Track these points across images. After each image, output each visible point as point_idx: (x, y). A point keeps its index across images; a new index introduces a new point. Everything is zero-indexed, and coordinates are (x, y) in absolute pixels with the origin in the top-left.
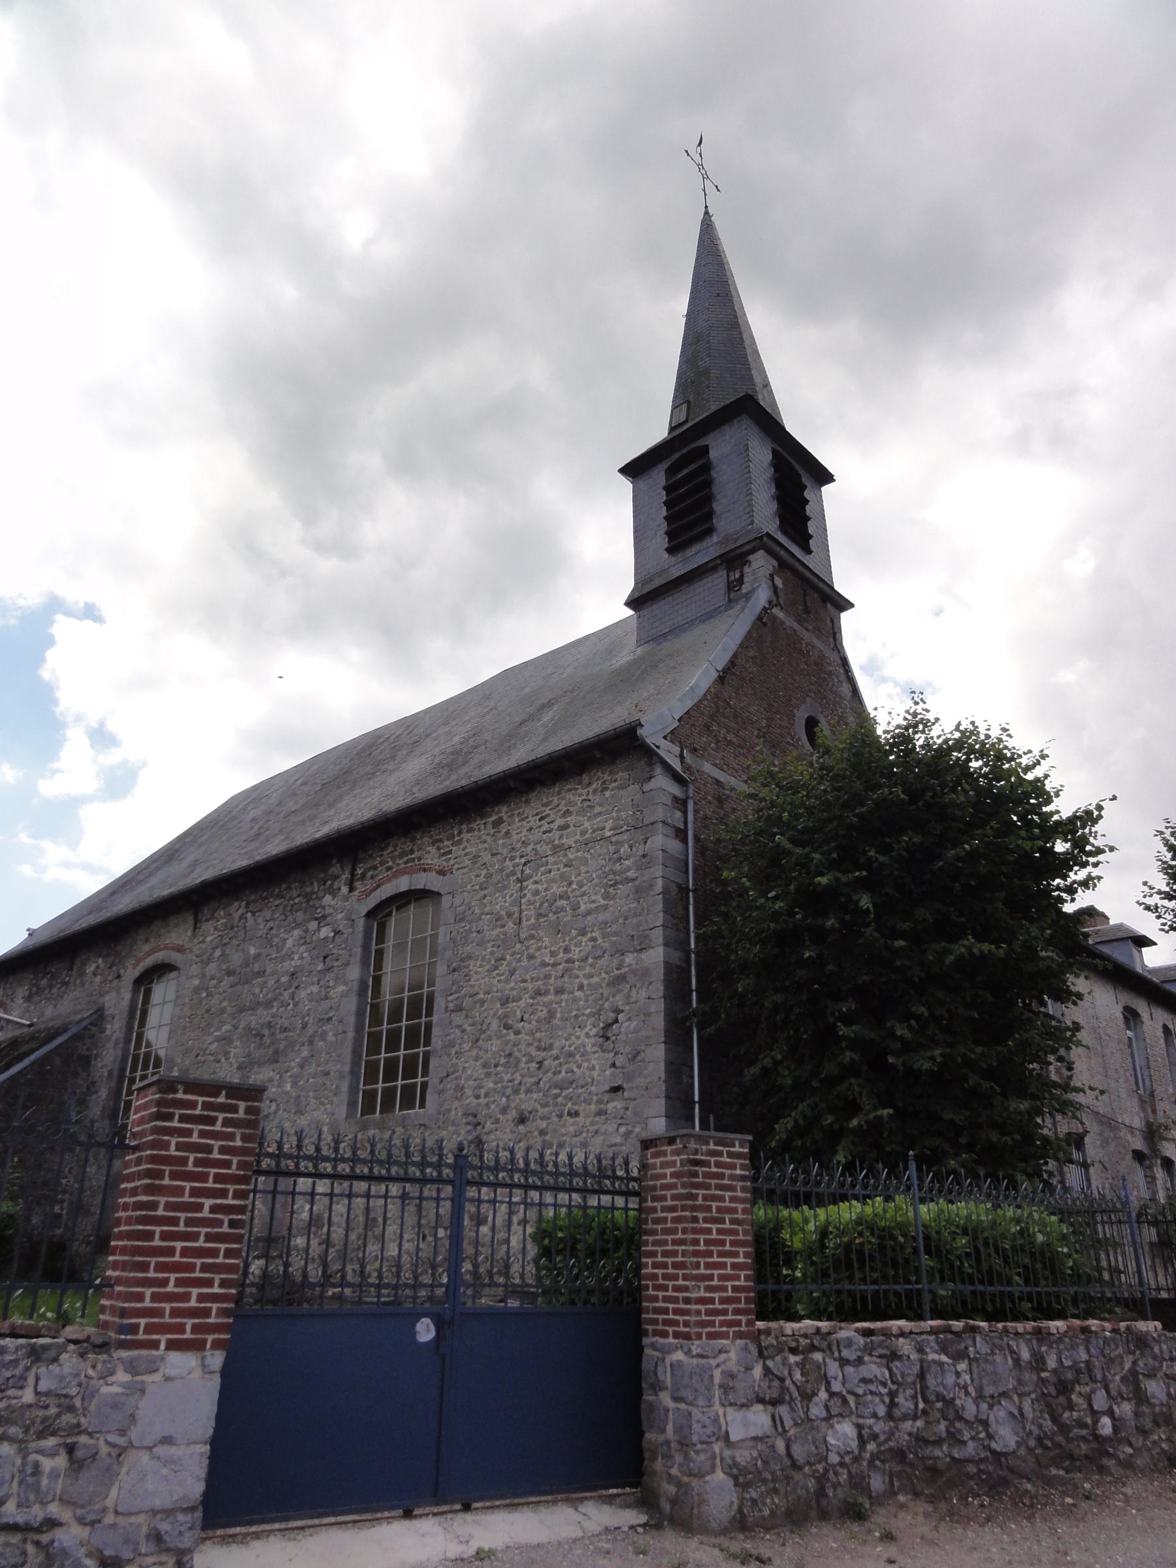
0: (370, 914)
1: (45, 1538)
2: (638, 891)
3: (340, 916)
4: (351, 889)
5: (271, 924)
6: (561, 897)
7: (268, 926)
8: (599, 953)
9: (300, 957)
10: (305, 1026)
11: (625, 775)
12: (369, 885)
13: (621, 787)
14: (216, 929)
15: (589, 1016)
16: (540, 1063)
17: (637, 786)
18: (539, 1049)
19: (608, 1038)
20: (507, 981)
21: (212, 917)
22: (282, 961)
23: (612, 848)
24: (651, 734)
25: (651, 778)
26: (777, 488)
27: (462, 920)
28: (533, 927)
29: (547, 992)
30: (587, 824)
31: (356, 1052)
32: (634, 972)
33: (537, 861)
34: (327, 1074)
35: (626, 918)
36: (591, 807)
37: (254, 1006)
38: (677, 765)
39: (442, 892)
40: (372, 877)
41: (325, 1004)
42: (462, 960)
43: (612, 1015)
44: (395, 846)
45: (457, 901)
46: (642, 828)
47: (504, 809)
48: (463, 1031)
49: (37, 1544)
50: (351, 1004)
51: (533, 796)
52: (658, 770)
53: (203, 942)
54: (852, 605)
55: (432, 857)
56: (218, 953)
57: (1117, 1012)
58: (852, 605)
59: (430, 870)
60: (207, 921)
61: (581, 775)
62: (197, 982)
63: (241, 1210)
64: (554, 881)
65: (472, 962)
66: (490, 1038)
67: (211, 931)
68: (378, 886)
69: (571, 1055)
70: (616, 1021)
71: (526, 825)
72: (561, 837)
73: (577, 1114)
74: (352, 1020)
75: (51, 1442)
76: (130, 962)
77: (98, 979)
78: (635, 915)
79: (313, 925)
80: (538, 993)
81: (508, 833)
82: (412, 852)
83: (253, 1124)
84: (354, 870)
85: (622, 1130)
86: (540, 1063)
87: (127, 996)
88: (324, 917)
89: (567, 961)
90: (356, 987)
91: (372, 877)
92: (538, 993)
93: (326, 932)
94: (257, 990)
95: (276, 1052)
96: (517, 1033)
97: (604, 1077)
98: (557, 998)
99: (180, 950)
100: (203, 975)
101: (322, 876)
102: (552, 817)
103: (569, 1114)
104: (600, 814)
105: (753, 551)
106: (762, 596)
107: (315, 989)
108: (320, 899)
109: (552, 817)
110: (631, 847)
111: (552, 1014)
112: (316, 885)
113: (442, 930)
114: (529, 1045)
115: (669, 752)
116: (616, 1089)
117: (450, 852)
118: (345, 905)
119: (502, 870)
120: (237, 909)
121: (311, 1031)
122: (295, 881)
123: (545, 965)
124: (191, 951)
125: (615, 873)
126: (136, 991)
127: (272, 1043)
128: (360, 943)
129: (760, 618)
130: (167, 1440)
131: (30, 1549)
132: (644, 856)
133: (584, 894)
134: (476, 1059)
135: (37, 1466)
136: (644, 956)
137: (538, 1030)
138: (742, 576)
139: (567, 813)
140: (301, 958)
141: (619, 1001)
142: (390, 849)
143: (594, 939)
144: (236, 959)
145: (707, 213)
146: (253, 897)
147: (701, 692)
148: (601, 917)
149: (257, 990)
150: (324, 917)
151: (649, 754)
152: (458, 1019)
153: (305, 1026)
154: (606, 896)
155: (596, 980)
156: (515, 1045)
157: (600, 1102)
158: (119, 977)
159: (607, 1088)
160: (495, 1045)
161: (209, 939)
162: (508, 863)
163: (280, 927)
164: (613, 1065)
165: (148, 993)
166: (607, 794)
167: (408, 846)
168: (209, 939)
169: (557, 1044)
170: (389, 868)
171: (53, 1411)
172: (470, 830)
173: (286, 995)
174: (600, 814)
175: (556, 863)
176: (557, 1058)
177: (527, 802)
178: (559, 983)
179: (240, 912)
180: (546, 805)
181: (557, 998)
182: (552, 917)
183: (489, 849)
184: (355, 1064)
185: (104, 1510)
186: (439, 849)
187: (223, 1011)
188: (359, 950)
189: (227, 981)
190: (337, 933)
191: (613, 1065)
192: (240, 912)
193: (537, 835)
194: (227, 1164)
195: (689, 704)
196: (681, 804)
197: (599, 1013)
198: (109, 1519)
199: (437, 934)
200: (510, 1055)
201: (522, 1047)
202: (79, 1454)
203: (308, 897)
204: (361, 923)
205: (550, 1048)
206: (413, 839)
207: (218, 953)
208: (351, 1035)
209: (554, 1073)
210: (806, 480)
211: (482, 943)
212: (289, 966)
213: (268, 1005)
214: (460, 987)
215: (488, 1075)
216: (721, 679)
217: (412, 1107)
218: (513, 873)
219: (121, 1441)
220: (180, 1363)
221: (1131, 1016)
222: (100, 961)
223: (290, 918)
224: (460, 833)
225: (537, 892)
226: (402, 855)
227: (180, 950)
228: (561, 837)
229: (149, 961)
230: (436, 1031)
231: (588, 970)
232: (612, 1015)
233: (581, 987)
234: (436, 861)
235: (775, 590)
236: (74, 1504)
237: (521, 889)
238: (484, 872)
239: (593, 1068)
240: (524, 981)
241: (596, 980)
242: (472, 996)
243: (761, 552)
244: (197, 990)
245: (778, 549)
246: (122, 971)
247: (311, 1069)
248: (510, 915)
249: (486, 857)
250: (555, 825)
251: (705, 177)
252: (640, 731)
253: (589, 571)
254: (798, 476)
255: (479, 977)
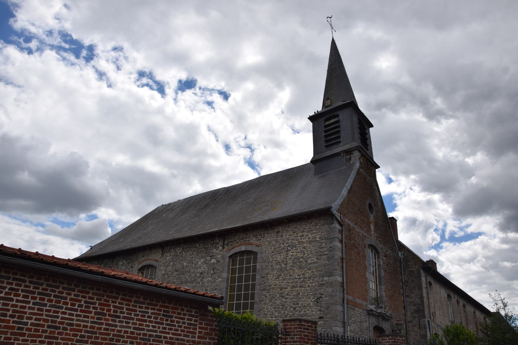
0: (230, 257)
2: (328, 258)
3: (219, 256)
4: (223, 248)
5: (192, 256)
6: (301, 258)
7: (191, 257)
8: (315, 276)
9: (204, 268)
13: (322, 225)
14: (170, 255)
15: (312, 295)
16: (295, 309)
18: (294, 304)
19: (318, 302)
20: (282, 282)
21: (169, 252)
22: (197, 268)
23: (319, 244)
25: (332, 224)
26: (360, 130)
27: (265, 262)
28: (291, 266)
29: (297, 287)
30: (310, 236)
32: (327, 283)
33: (293, 246)
35: (324, 266)
36: (312, 231)
38: (339, 219)
40: (231, 245)
42: (266, 274)
44: (240, 236)
45: (263, 256)
46: (331, 239)
47: (280, 228)
48: (266, 297)
50: (224, 285)
52: (335, 221)
53: (166, 259)
55: (253, 240)
56: (171, 264)
57: (446, 295)
60: (167, 252)
64: (299, 252)
67: (168, 257)
68: (233, 248)
70: (321, 297)
71: (288, 235)
72: (301, 239)
74: (225, 290)
77: (124, 267)
78: (328, 265)
79: (209, 258)
80: (294, 287)
81: (282, 236)
82: (246, 238)
84: (224, 242)
85: (323, 330)
86: (295, 309)
89: (304, 278)
91: (231, 245)
92: (294, 287)
93: (213, 261)
94: (188, 277)
96: (286, 299)
99: (157, 261)
104: (315, 233)
105: (354, 150)
106: (358, 165)
107: (210, 279)
108: (211, 250)
110: (326, 244)
111: (298, 294)
112: (209, 245)
113: (258, 264)
115: (338, 215)
116: (321, 318)
117: (260, 240)
118: (221, 253)
119: (280, 247)
120: (179, 250)
123: (296, 278)
125: (321, 252)
128: (227, 266)
129: (357, 172)
133: (309, 258)
134: (271, 306)
136: (330, 278)
137: (293, 298)
138: (350, 158)
139: (303, 232)
140: (204, 268)
142: (238, 236)
143: (313, 272)
144: (178, 266)
146: (185, 247)
147: (344, 196)
150: (213, 256)
151: (332, 215)
152: (264, 293)
154: (317, 259)
155: (314, 284)
158: (132, 267)
159: (318, 317)
161: (167, 259)
162: (282, 245)
163: (195, 257)
164: (320, 310)
166: (317, 227)
167: (244, 236)
168: (167, 259)
169: (300, 303)
170: (237, 243)
172: (268, 233)
173: (199, 280)
174: (315, 233)
176: (300, 307)
177: (289, 227)
178: (301, 284)
179: (180, 251)
180: (296, 228)
183: (275, 240)
186: (256, 238)
189: (175, 273)
190: (218, 261)
192: (180, 251)
194: (312, 340)
195: (342, 200)
196: (341, 232)
197: (315, 294)
200: (284, 305)
203: (207, 249)
204: (227, 259)
205: (297, 304)
207: (171, 264)
210: (366, 127)
211: (273, 270)
212: (200, 270)
213: (192, 282)
214: (265, 283)
215: (276, 311)
218: (284, 249)
221: (449, 296)
223: (200, 255)
224: (264, 234)
225: (292, 256)
226: (242, 239)
227: (157, 261)
228: (301, 239)
229: (144, 263)
230: (256, 296)
231: (311, 281)
233: (309, 286)
234: (255, 242)
235: (361, 163)
237: (287, 254)
238: (273, 247)
239: (313, 311)
240: (289, 283)
241: (314, 284)
242: (269, 286)
243: (357, 151)
244: (164, 275)
245: (361, 150)
246: (133, 266)
249: (274, 243)
253: (298, 149)
254: (364, 124)
255: (271, 280)
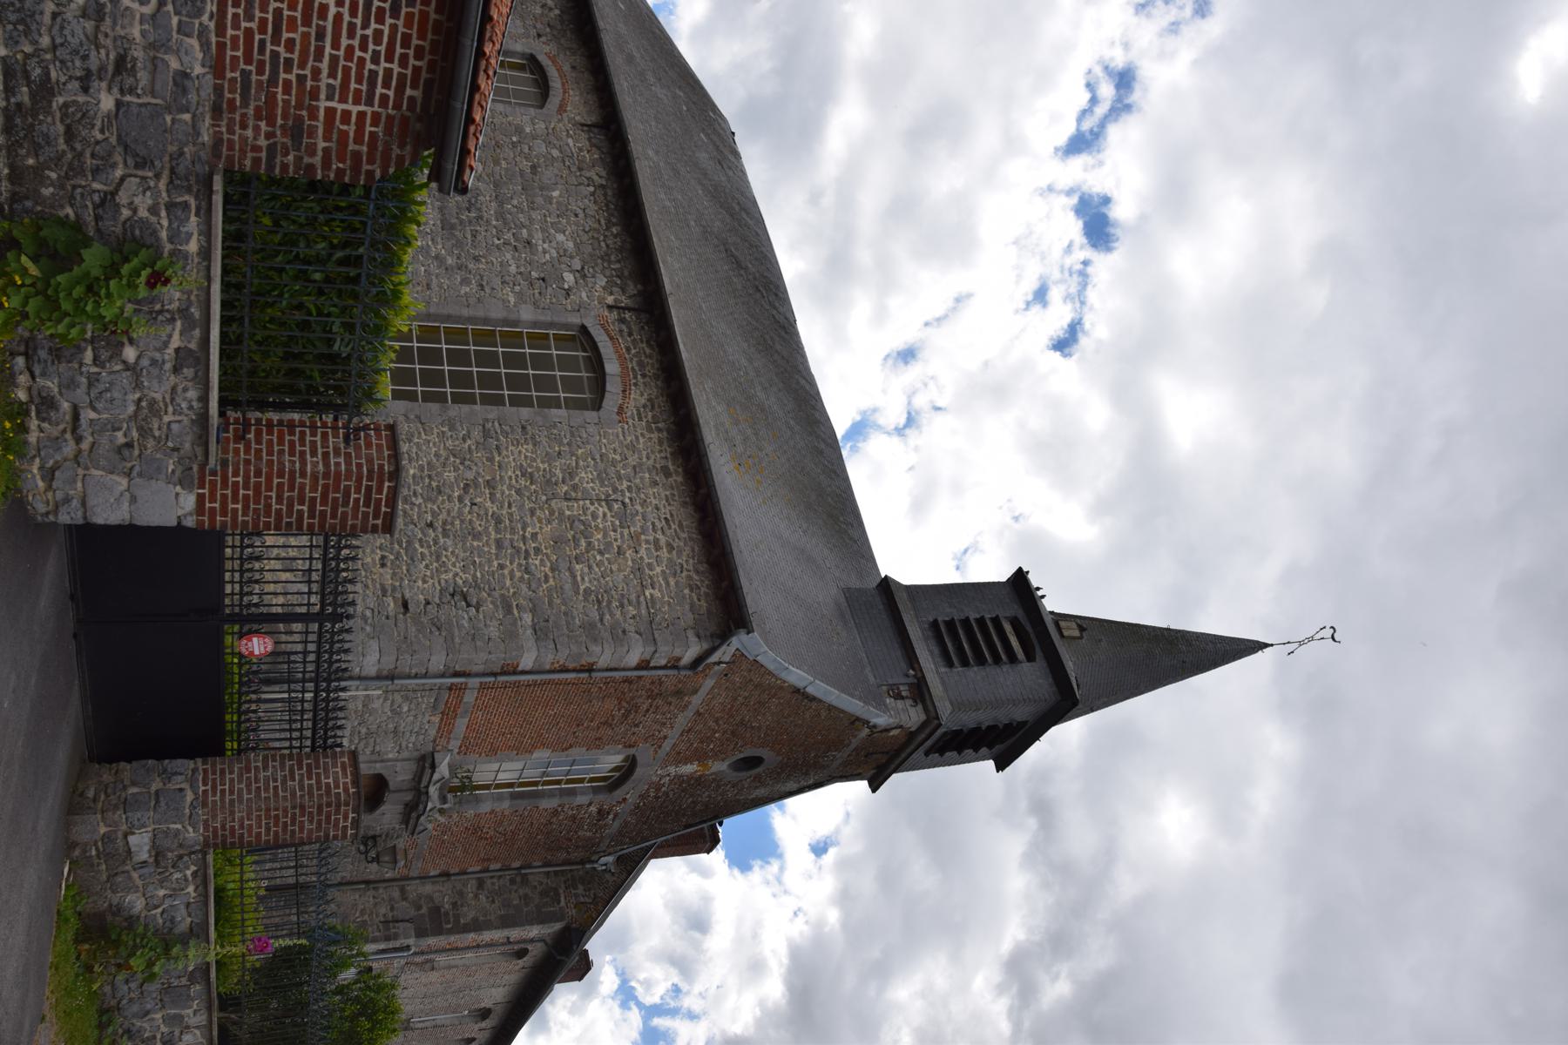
0: (584, 329)
1: (68, 436)
2: (592, 625)
3: (584, 295)
4: (610, 307)
5: (581, 215)
6: (589, 544)
7: (579, 211)
8: (534, 586)
9: (546, 251)
10: (476, 259)
11: (704, 610)
12: (614, 328)
13: (692, 605)
14: (581, 150)
15: (474, 576)
16: (430, 525)
17: (691, 623)
18: (445, 523)
19: (453, 595)
20: (510, 487)
21: (592, 145)
22: (543, 230)
23: (633, 597)
24: (738, 641)
25: (698, 636)
26: (989, 728)
27: (572, 435)
28: (561, 513)
29: (498, 531)
30: (658, 569)
31: (448, 318)
32: (514, 623)
33: (624, 518)
34: (428, 286)
35: (566, 614)
36: (675, 575)
37: (500, 200)
38: (714, 658)
39: (602, 412)
40: (621, 331)
41: (498, 281)
42: (533, 437)
43: (474, 601)
44: (650, 357)
45: (591, 429)
46: (649, 633)
47: (680, 479)
48: (464, 440)
49: (64, 431)
50: (497, 313)
51: (690, 509)
52: (706, 646)
53: (568, 135)
54: (874, 790)
55: (637, 398)
56: (555, 153)
57: (487, 1003)
58: (874, 790)
59: (624, 397)
60: (589, 139)
61: (708, 562)
62: (528, 130)
63: (300, 527)
64: (605, 535)
65: (530, 447)
66: (456, 469)
67: (577, 143)
68: (611, 338)
69: (438, 558)
70: (469, 605)
71: (659, 503)
72: (647, 542)
73: (383, 565)
74: (480, 313)
75: (135, 434)
76: (550, 48)
77: (538, 11)
78: (568, 623)
79: (577, 265)
80: (498, 521)
81: (655, 483)
82: (644, 376)
83: (365, 531)
84: (629, 309)
85: (368, 613)
86: (430, 525)
87: (519, 47)
88: (584, 277)
89: (527, 551)
90: (513, 317)
91: (621, 331)
92: (498, 521)
93: (569, 278)
94: (515, 202)
95: (453, 227)
96: (460, 499)
97: (416, 596)
98: (492, 542)
99: (562, 109)
100: (534, 137)
101: (626, 273)
102: (668, 532)
103: (383, 557)
104: (668, 584)
105: (926, 710)
106: (881, 720)
107: (513, 269)
108: (602, 272)
109: (668, 532)
110: (634, 617)
111: (477, 536)
112: (617, 266)
113: (563, 412)
114: (449, 512)
115: (725, 653)
116: (405, 605)
117: (640, 419)
118: (594, 300)
119: (620, 478)
120: (598, 174)
121: (471, 266)
122: (623, 242)
123: (524, 529)
124: (560, 121)
125: (609, 602)
126: (523, 55)
127: (461, 222)
128: (556, 319)
129: (858, 719)
130: (133, 500)
131: (61, 427)
132: (624, 632)
133: (590, 567)
134: (437, 455)
135: (119, 429)
136: (529, 632)
137: (462, 521)
138: (903, 698)
139: (670, 547)
140: (545, 252)
141: (488, 607)
142: (648, 351)
143: (546, 581)
144: (548, 175)
145: (1266, 645)
146: (610, 193)
147: (783, 675)
148: (568, 587)
149: (515, 202)
150: (584, 277)
151: (723, 636)
152: (477, 433)
153: (476, 259)
154: (587, 592)
155: (508, 583)
156: (449, 497)
157: (394, 589)
158: (539, 36)
159: (407, 596)
160: (450, 475)
161: (570, 141)
162: (625, 484)
163: (577, 224)
164: (428, 603)
165: (521, 68)
166: (687, 591)
167: (650, 371)
168: (570, 141)
169: (449, 543)
170: (628, 349)
171: (157, 433)
172: (660, 442)
173: (508, 236)
174: (668, 584)
175: (622, 535)
176: (436, 543)
177: (684, 504)
178: (507, 543)
179: (596, 178)
180: (680, 526)
181: (492, 542)
182: (570, 535)
183: (641, 465)
184: (436, 317)
185: (87, 468)
186: (644, 406)
187: (497, 162)
188: (549, 319)
189: (526, 165)
190: (568, 292)
191: (428, 603)
192: (596, 178)
193: (651, 516)
194: (334, 516)
195: (771, 667)
196: (674, 665)
197: (477, 586)
198: (81, 472)
199: (559, 407)
200: (440, 492)
201: (447, 505)
202: (126, 452)
203: (605, 257)
204: (575, 320)
205: (445, 534)
206: (656, 377)
207: (555, 153)
208: (465, 312)
209: (420, 540)
210: (998, 748)
211: (548, 458)
212: (538, 238)
213: (500, 215)
214: (506, 435)
215: (421, 468)
216: (797, 691)
217: (394, 382)
218: (615, 490)
219: (134, 473)
220: (189, 501)
221: (484, 1014)
222: (557, 12)
223: (585, 238)
224: (659, 430)
225: (594, 516)
226: (641, 364)
227: (562, 109)
228: (647, 542)
229: (552, 72)
230: (465, 408)
231: (518, 574)
232: (474, 601)
233: (501, 567)
234: (632, 403)
235: (887, 730)
236: (91, 451)
237: (599, 500)
238: (618, 457)
239: (425, 582)
240: (510, 506)
241: (508, 583)
242: (498, 448)
243: (923, 717)
244: (519, 130)
245: (927, 731)
246: (543, 39)
247: (434, 269)
248: (575, 488)
249: (633, 460)
250: (660, 536)
251: (1301, 643)
252: (742, 632)
253: (922, 538)
254: (1005, 742)
255: (516, 454)
